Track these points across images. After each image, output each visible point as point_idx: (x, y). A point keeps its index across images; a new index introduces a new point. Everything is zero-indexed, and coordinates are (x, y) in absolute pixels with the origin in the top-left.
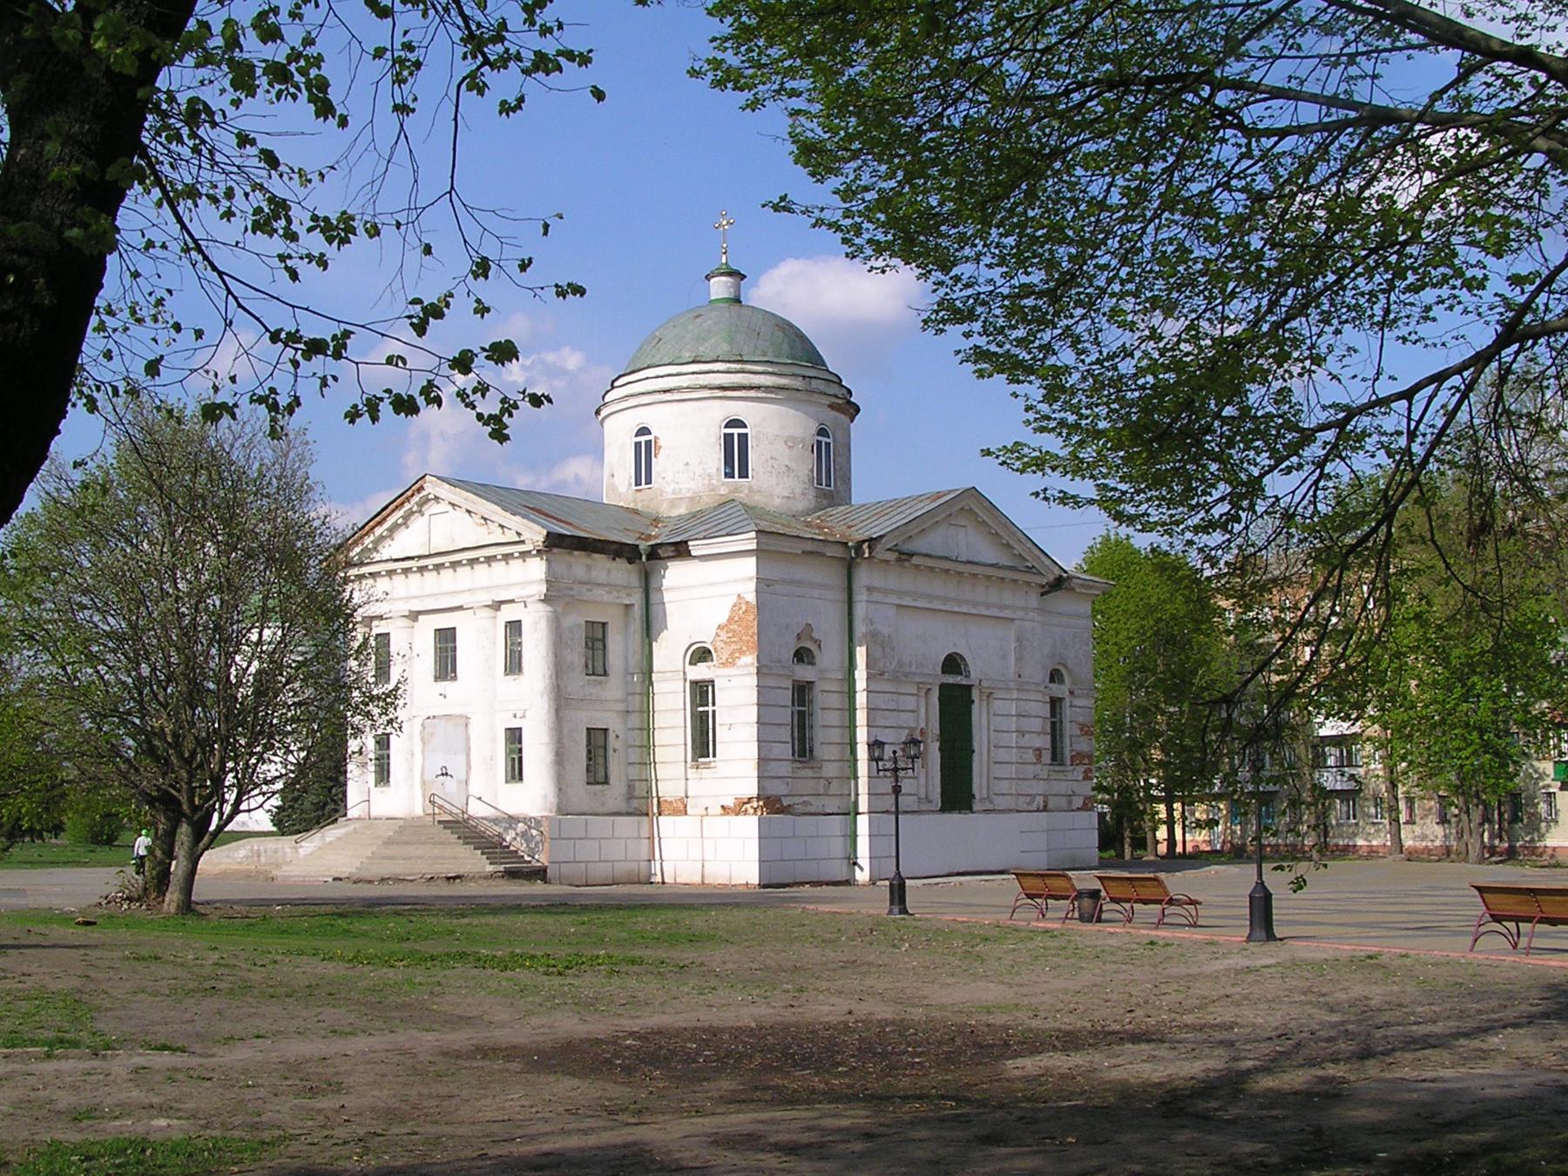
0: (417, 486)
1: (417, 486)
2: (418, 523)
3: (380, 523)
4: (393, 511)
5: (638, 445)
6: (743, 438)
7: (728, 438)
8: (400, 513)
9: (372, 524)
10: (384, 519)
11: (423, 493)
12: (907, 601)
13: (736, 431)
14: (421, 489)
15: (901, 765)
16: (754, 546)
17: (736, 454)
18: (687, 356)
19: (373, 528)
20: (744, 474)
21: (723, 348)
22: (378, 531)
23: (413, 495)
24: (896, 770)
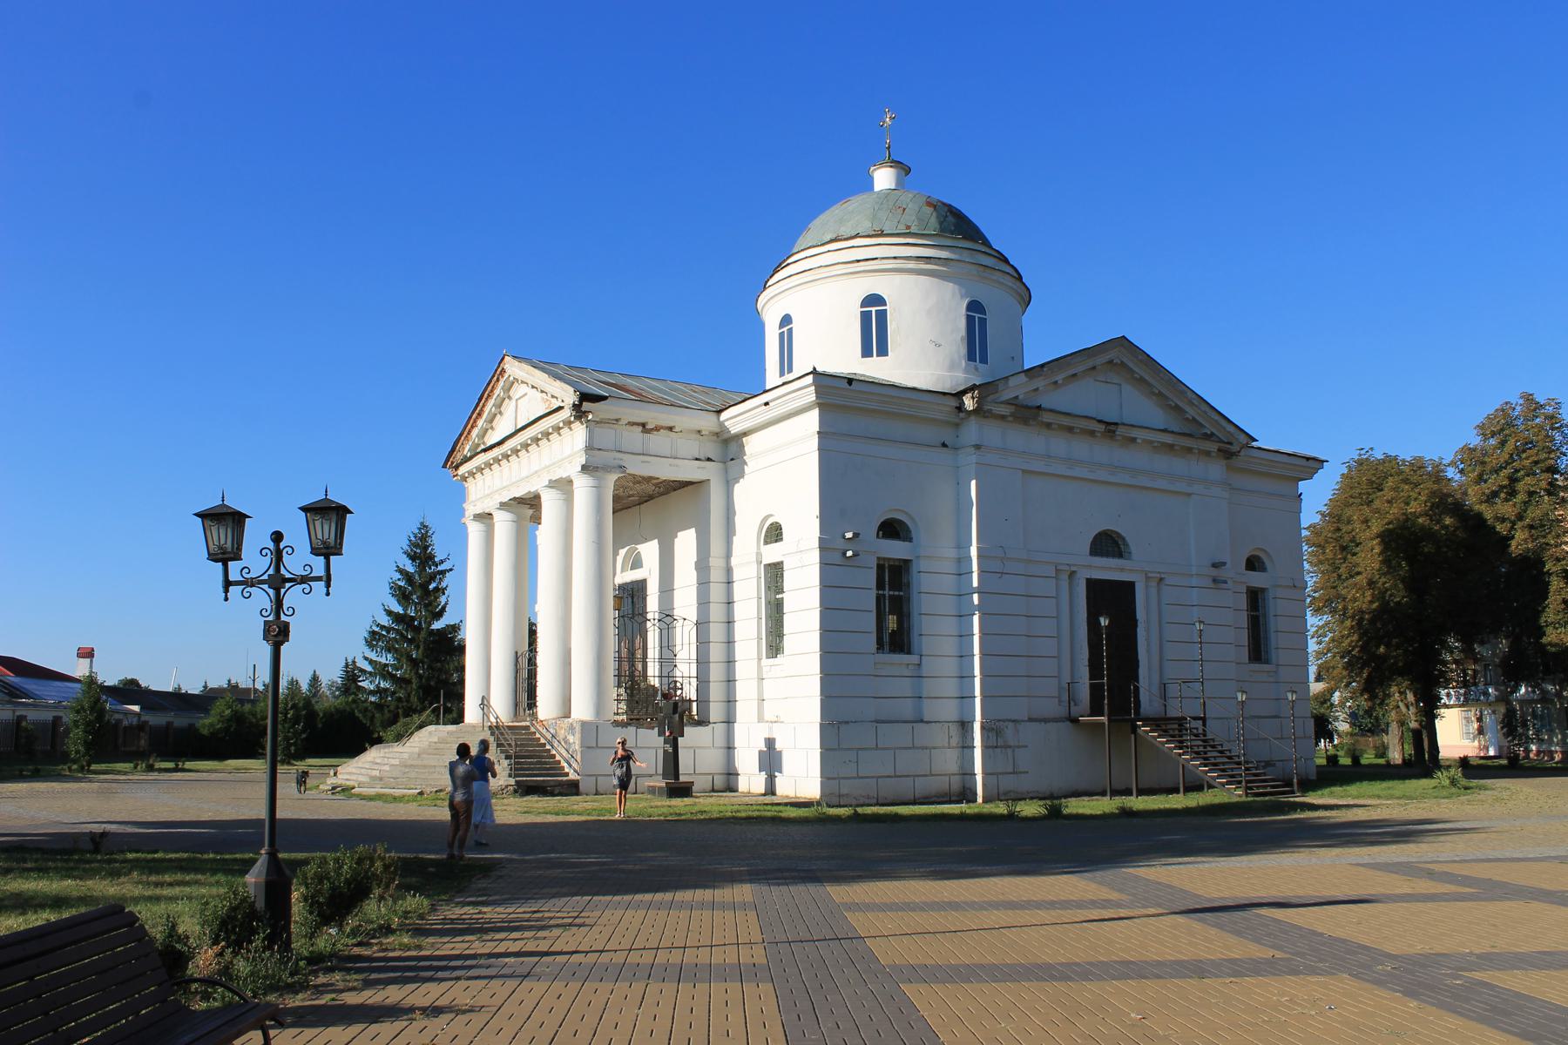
0: (500, 369)
1: (500, 369)
2: (508, 408)
3: (480, 415)
4: (487, 399)
5: (781, 335)
6: (882, 316)
7: (866, 318)
8: (491, 402)
9: (474, 416)
10: (482, 410)
11: (506, 376)
12: (1037, 466)
13: (873, 309)
14: (503, 371)
15: (294, 564)
16: (813, 397)
17: (874, 335)
18: (828, 238)
19: (475, 422)
20: (883, 351)
21: (866, 226)
22: (480, 423)
23: (498, 380)
24: (278, 582)
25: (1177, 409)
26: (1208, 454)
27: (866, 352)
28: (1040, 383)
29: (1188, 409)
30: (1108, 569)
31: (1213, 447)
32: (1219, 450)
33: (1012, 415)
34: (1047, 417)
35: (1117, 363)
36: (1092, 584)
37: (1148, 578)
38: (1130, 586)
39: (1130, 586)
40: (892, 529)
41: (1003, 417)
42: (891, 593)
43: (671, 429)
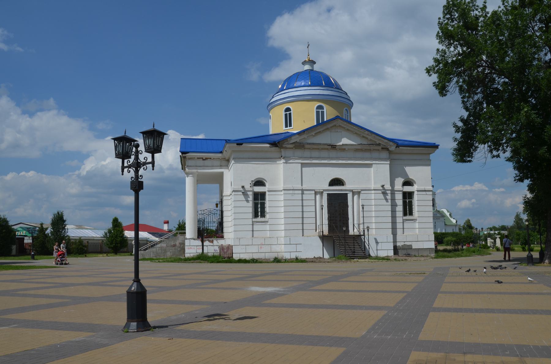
13: (288, 113)
20: (290, 126)
25: (363, 137)
26: (378, 150)
27: (286, 126)
28: (305, 136)
29: (368, 136)
30: (337, 189)
31: (380, 148)
32: (382, 148)
33: (294, 147)
34: (307, 146)
35: (337, 126)
36: (328, 195)
37: (354, 193)
38: (347, 194)
39: (347, 194)
40: (259, 183)
41: (292, 148)
42: (258, 201)
43: (211, 158)
